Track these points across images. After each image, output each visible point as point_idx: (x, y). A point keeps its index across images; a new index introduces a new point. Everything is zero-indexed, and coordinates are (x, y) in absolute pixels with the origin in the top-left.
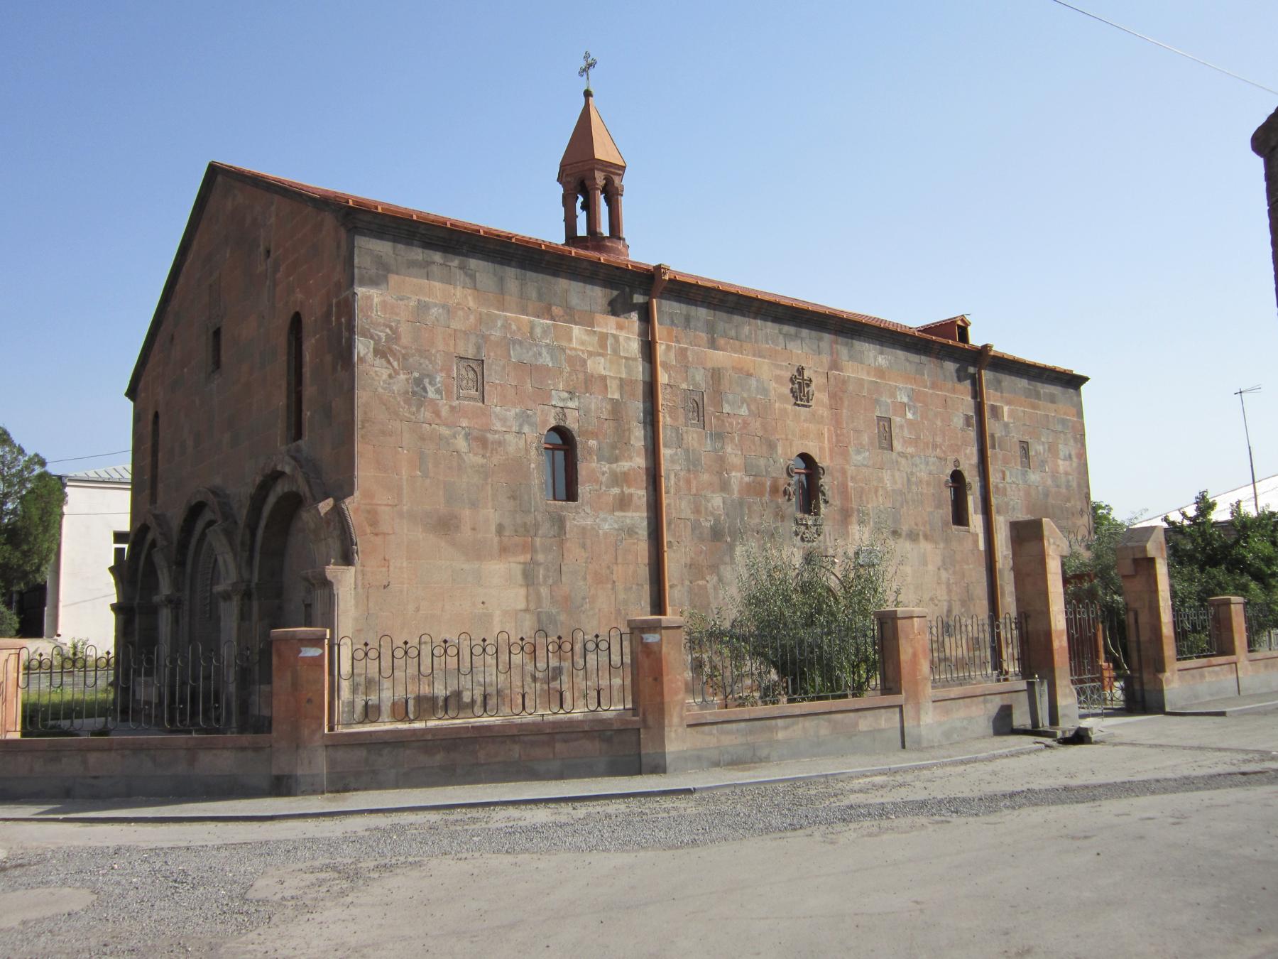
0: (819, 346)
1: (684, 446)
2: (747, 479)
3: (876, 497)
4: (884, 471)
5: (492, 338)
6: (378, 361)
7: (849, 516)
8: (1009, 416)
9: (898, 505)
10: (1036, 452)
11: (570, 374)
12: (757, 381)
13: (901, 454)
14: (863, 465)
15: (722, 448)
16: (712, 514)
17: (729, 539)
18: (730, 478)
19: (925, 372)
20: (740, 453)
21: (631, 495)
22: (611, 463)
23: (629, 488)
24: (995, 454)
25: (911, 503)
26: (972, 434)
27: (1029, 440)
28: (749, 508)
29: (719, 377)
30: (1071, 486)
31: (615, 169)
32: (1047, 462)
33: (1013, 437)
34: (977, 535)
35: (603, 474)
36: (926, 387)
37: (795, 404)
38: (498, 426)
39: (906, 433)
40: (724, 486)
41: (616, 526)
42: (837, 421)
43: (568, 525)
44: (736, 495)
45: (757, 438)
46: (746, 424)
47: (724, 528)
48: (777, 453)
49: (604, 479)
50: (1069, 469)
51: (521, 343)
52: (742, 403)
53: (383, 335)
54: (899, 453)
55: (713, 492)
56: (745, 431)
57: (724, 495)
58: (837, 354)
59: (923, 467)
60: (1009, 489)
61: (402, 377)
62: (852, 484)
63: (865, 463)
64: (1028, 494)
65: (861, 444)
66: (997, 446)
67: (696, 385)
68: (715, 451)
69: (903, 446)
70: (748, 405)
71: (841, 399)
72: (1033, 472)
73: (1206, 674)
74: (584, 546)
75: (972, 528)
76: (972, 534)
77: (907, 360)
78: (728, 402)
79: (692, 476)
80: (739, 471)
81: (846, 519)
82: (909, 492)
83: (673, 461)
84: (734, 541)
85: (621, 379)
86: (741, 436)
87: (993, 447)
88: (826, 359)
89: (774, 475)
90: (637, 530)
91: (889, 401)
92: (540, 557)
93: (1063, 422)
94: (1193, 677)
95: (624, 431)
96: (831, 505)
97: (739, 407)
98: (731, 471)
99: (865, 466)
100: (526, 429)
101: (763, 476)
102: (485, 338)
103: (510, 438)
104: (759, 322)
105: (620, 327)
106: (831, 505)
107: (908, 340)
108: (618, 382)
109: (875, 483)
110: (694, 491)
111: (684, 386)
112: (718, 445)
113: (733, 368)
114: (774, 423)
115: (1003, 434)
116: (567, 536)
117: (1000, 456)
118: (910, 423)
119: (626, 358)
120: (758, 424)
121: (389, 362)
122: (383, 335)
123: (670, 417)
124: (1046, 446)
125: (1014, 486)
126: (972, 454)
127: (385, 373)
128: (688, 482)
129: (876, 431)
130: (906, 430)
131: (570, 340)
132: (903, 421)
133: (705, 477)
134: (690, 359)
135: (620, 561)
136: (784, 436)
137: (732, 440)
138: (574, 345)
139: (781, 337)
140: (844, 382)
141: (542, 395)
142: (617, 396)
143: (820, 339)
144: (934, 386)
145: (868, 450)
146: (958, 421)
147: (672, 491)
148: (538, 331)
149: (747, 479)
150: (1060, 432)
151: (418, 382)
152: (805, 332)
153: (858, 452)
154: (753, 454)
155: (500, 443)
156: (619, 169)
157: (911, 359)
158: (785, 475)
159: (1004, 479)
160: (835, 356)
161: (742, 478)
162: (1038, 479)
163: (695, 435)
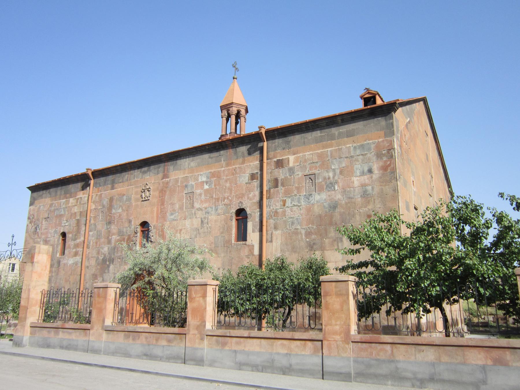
0: (158, 171)
1: (97, 230)
2: (118, 238)
3: (180, 233)
5: (52, 210)
6: (30, 225)
8: (294, 162)
9: (193, 236)
10: (325, 178)
11: (67, 214)
12: (127, 196)
13: (200, 209)
14: (174, 220)
15: (110, 227)
16: (104, 254)
17: (108, 263)
18: (111, 239)
19: (222, 159)
20: (116, 228)
21: (78, 251)
22: (74, 241)
23: (78, 248)
24: (278, 191)
25: (202, 234)
26: (256, 183)
27: (317, 172)
28: (117, 249)
29: (112, 200)
30: (368, 195)
31: (230, 105)
32: (336, 182)
33: (298, 175)
34: (253, 246)
35: (72, 245)
36: (222, 167)
37: (143, 201)
38: (50, 236)
39: (203, 197)
40: (109, 242)
41: (73, 262)
42: (162, 202)
43: (61, 263)
44: (113, 245)
46: (120, 215)
47: (107, 259)
49: (72, 247)
50: (367, 181)
51: (57, 209)
52: (120, 208)
53: (31, 217)
54: (197, 209)
55: (105, 245)
57: (108, 246)
58: (167, 170)
59: (213, 212)
60: (288, 210)
61: (33, 227)
64: (309, 210)
65: (174, 210)
66: (279, 184)
67: (104, 206)
68: (108, 229)
69: (200, 204)
70: (122, 208)
71: (165, 191)
72: (319, 194)
73: (61, 333)
74: (64, 270)
75: (249, 242)
76: (249, 246)
77: (210, 157)
78: (114, 209)
79: (98, 240)
82: (201, 228)
83: (93, 236)
84: (110, 264)
85: (81, 212)
86: (117, 221)
87: (276, 186)
88: (161, 175)
89: (129, 234)
90: (78, 263)
91: (193, 183)
92: (53, 274)
93: (362, 147)
94: (49, 332)
95: (79, 229)
96: (154, 242)
97: (119, 209)
98: (112, 236)
99: (176, 220)
100: (56, 235)
101: (125, 235)
102: (50, 211)
103: (52, 239)
104: (132, 172)
105: (84, 194)
106: (154, 242)
107: (207, 148)
108: (79, 213)
109: (180, 228)
110: (98, 246)
111: (100, 208)
112: (108, 227)
113: (118, 195)
115: (288, 175)
116: (60, 267)
117: (283, 191)
118: (206, 191)
119: (83, 204)
120: (125, 214)
121: (32, 224)
122: (31, 217)
123: (94, 220)
124: (338, 171)
125: (295, 208)
126: (255, 196)
127: (30, 227)
128: (96, 243)
129: (184, 201)
130: (203, 195)
131: (69, 204)
132: (202, 191)
133: (102, 240)
134: (103, 197)
135: (72, 274)
137: (114, 223)
138: (70, 205)
139: (141, 174)
140: (167, 183)
141: (60, 224)
142: (79, 218)
143: (159, 168)
144: (228, 165)
146: (245, 178)
147: (91, 247)
148: (62, 203)
150: (358, 156)
151: (36, 228)
152: (152, 167)
153: (172, 214)
154: (121, 227)
155: (49, 241)
156: (231, 105)
157: (211, 156)
158: (134, 233)
159: (284, 205)
160: (166, 172)
161: (116, 238)
162: (325, 197)
163: (101, 225)
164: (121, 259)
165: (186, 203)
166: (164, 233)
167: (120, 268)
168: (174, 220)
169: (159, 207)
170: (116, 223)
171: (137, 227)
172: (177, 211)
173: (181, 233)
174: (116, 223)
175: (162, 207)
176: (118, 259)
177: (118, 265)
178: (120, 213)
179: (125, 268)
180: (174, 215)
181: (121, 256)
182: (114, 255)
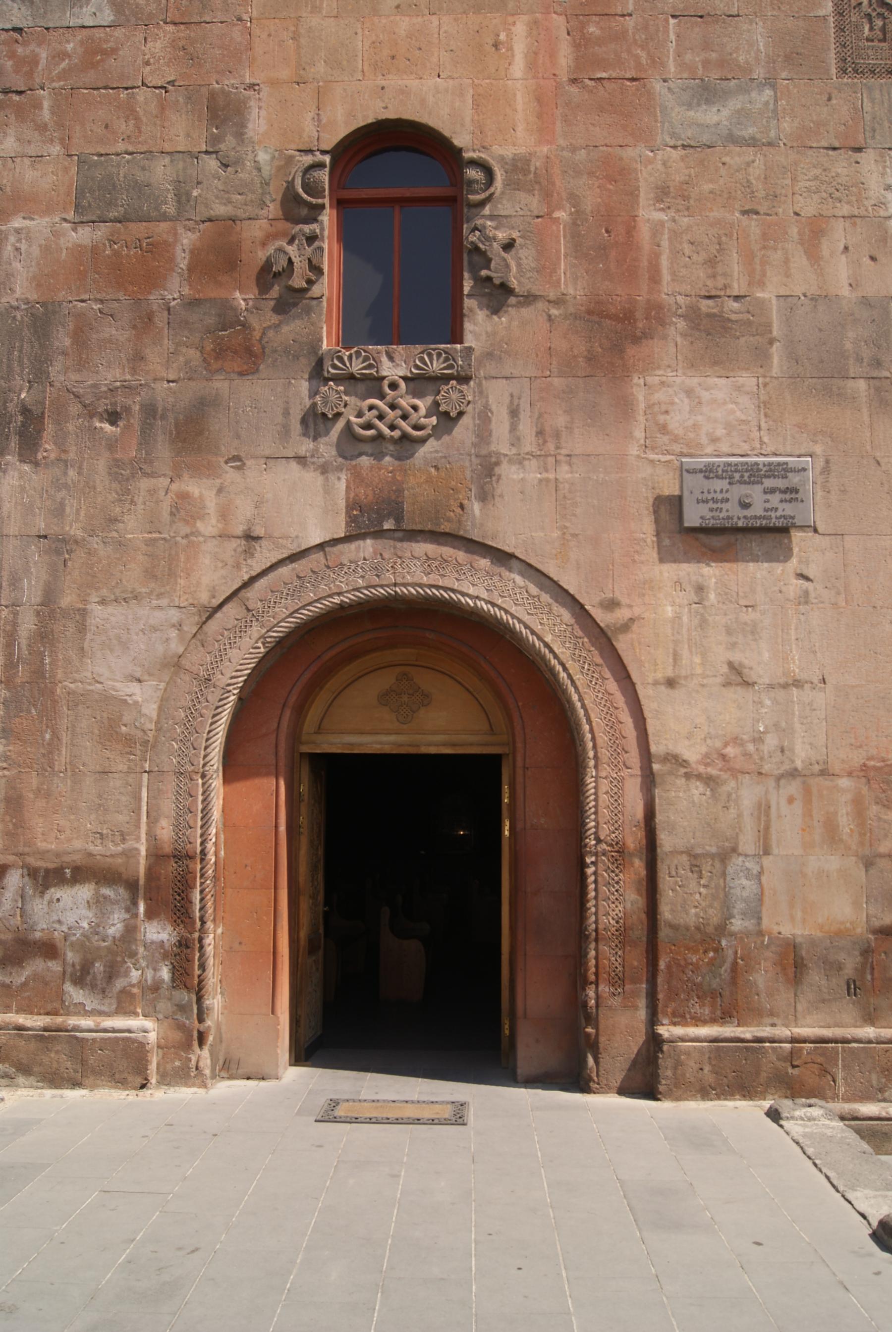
2: (84, 236)
4: (868, 158)
7: (636, 340)
14: (732, 139)
20: (56, 149)
28: (80, 337)
45: (142, 95)
48: (240, 135)
56: (90, 77)
62: (662, 216)
63: (750, 131)
80: (48, 211)
81: (618, 349)
89: (220, 210)
99: (752, 142)
101: (164, 217)
106: (530, 299)
114: (236, 33)
120: (157, 47)
136: (285, 73)
145: (771, 82)
149: (84, 236)
161: (56, 234)
164: (136, 422)
165: (840, 29)
166: (631, 228)
167: (125, 495)
168: (732, 139)
169: (559, 22)
170: (46, 114)
171: (308, 159)
172: (759, 73)
173: (825, 251)
174: (46, 114)
175: (592, 29)
176: (91, 415)
177: (101, 465)
178: (99, 34)
179: (184, 496)
180: (735, 103)
181: (128, 388)
182: (39, 376)
